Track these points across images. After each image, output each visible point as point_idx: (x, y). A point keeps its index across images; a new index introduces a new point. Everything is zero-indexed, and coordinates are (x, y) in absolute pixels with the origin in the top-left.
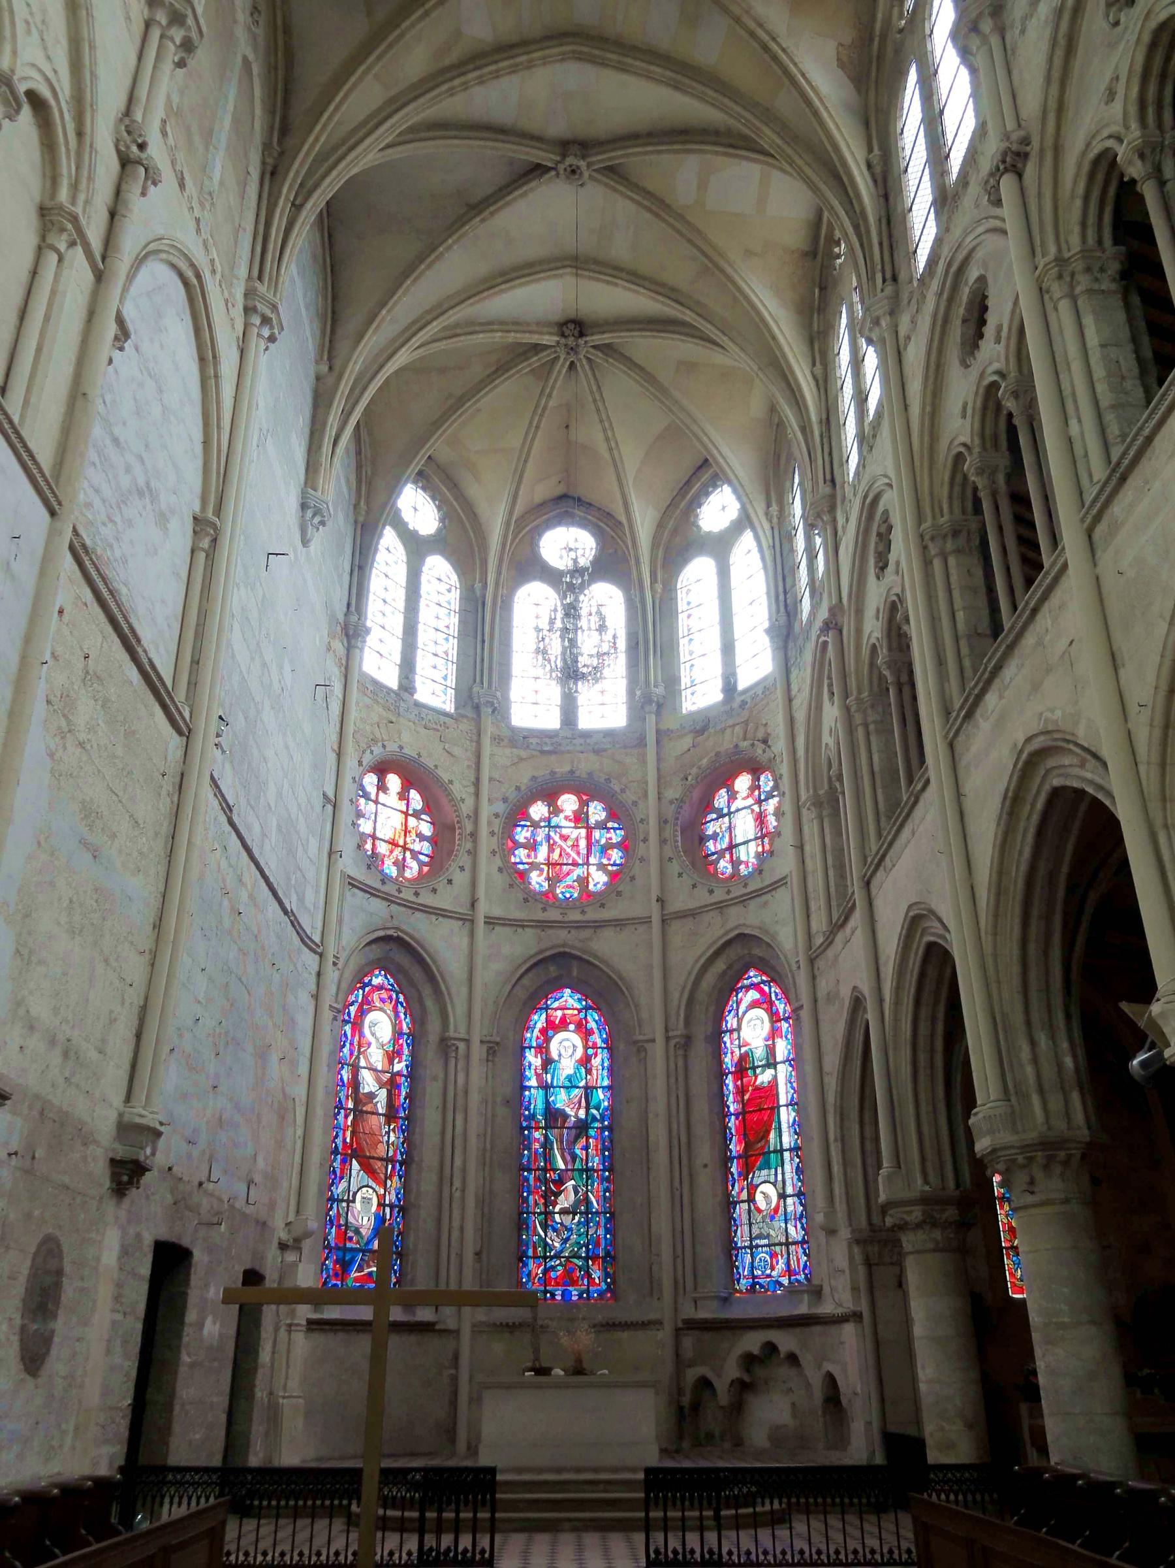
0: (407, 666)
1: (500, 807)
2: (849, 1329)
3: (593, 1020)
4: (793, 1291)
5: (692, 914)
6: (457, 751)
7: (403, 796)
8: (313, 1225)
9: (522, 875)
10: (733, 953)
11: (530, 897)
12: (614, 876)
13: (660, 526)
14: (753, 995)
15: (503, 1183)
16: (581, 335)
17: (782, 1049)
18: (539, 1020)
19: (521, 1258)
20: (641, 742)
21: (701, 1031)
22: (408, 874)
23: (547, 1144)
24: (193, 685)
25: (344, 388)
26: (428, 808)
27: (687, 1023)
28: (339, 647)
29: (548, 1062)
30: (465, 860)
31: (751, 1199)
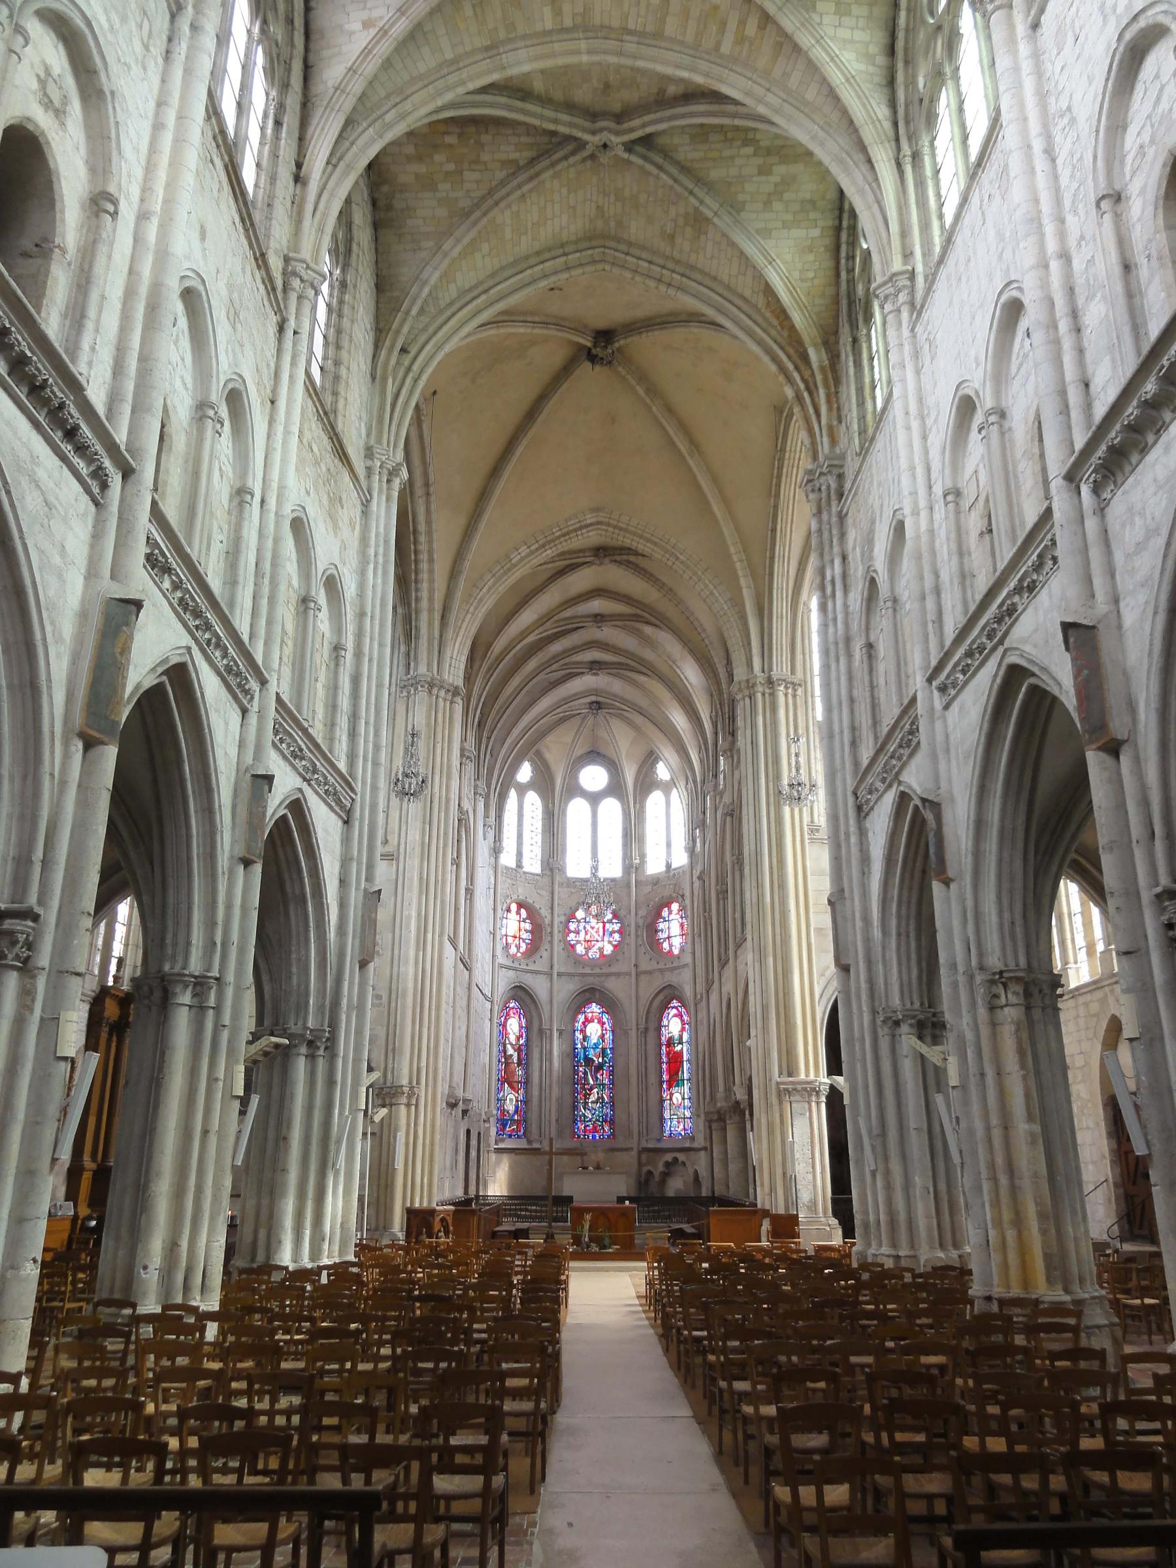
0: (519, 854)
1: (563, 919)
2: (702, 1153)
3: (605, 1018)
4: (684, 1138)
5: (650, 973)
6: (543, 893)
7: (518, 913)
8: (495, 1112)
9: (573, 947)
10: (666, 992)
11: (578, 961)
12: (615, 947)
13: (639, 772)
14: (674, 1011)
15: (567, 1090)
16: (600, 708)
17: (685, 1037)
18: (581, 1018)
19: (575, 1121)
20: (628, 885)
21: (652, 1026)
22: (522, 950)
23: (585, 1073)
24: (470, 950)
25: (498, 766)
26: (529, 917)
27: (646, 1022)
28: (493, 860)
29: (585, 1038)
30: (547, 946)
31: (671, 1099)
